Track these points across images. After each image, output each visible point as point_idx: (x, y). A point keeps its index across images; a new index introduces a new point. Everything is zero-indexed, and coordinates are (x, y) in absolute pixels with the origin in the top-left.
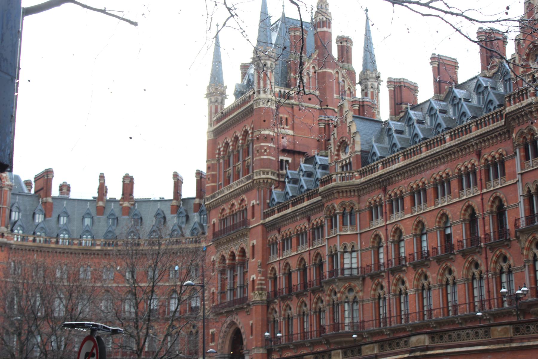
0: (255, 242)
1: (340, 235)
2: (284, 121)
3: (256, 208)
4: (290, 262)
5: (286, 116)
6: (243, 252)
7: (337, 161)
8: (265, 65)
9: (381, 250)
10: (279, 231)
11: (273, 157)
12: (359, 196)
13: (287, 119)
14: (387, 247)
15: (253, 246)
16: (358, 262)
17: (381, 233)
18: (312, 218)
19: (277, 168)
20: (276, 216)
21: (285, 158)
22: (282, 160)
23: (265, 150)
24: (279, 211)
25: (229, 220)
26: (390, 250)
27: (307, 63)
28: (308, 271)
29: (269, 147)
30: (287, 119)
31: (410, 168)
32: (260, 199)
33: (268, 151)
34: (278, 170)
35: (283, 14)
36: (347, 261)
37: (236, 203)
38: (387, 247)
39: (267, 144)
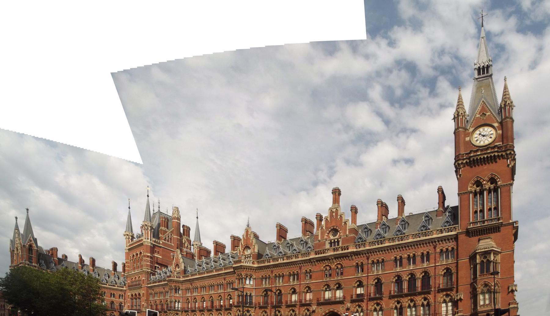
0: (144, 292)
1: (174, 296)
3: (144, 280)
4: (157, 301)
6: (139, 294)
7: (175, 271)
9: (190, 304)
10: (153, 290)
14: (191, 303)
15: (143, 293)
16: (181, 306)
17: (189, 298)
18: (165, 288)
20: (152, 285)
24: (153, 283)
25: (134, 282)
26: (192, 304)
28: (163, 305)
32: (146, 278)
36: (177, 305)
37: (137, 277)
38: (191, 303)
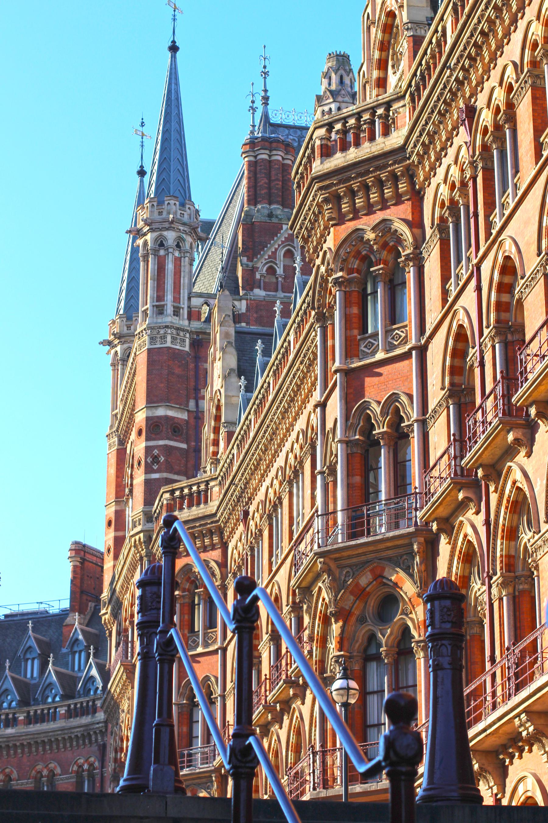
8: (162, 245)
12: (224, 546)
23: (155, 459)
29: (168, 450)
33: (162, 459)
35: (266, 117)
39: (161, 443)
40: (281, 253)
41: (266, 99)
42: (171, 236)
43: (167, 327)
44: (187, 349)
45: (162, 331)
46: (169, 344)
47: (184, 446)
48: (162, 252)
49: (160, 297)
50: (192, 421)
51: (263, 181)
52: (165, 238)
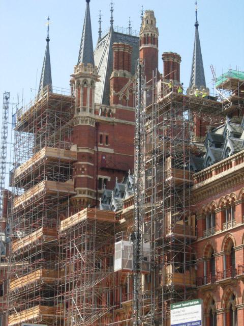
2: (104, 139)
5: (106, 134)
8: (85, 83)
11: (91, 176)
13: (107, 137)
19: (95, 187)
21: (104, 177)
22: (100, 179)
23: (83, 169)
27: (130, 80)
29: (88, 166)
30: (107, 137)
31: (203, 191)
33: (86, 169)
34: (97, 189)
35: (112, 28)
40: (128, 92)
41: (112, 21)
42: (89, 80)
43: (88, 117)
44: (94, 126)
45: (86, 119)
46: (88, 124)
47: (93, 165)
48: (85, 86)
49: (85, 104)
50: (96, 155)
51: (121, 60)
52: (87, 81)
